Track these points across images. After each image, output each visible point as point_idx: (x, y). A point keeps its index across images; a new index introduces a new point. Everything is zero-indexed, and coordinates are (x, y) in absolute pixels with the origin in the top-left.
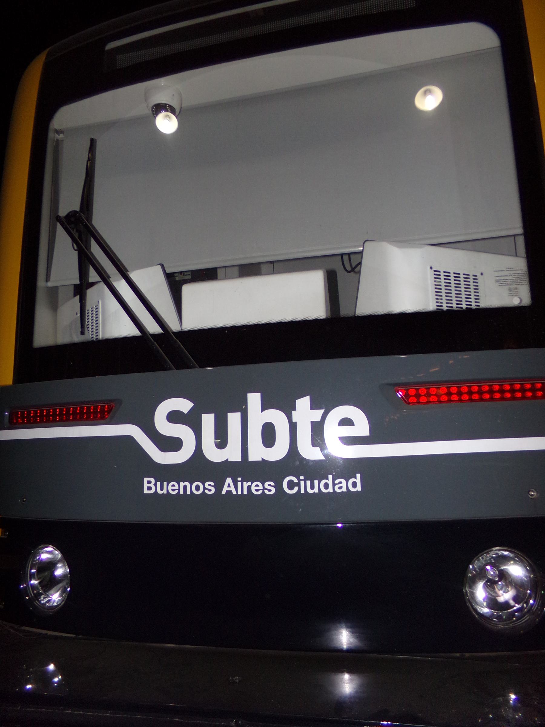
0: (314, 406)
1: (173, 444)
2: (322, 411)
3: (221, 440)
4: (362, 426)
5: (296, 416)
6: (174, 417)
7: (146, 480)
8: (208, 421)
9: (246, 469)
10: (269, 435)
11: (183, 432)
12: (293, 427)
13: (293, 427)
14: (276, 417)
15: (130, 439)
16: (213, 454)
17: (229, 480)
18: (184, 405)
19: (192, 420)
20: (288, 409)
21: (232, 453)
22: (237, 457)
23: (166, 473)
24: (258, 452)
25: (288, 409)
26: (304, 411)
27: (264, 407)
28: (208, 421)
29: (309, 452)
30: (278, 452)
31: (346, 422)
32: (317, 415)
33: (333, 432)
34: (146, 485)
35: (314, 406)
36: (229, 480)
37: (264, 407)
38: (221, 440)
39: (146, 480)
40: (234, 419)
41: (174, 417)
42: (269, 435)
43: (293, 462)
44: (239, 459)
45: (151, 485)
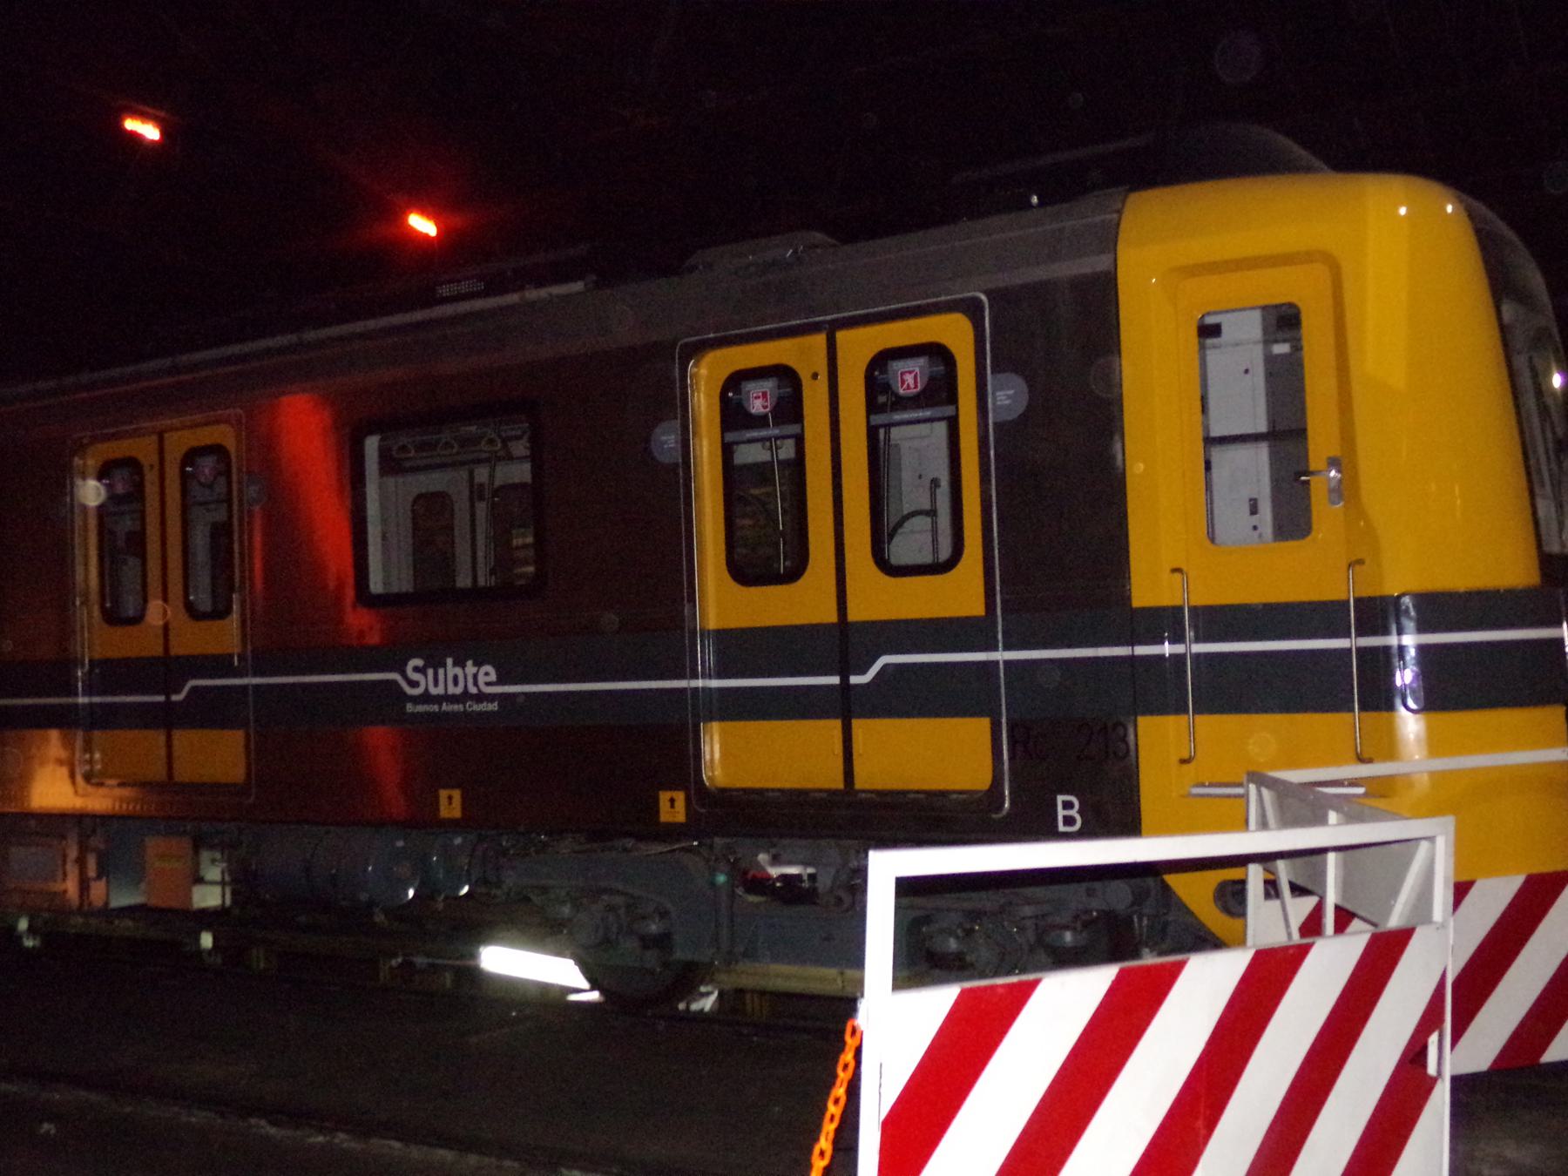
1: (414, 684)
3: (436, 683)
4: (493, 677)
6: (416, 669)
8: (430, 672)
9: (448, 698)
14: (458, 671)
15: (395, 682)
16: (433, 691)
18: (418, 662)
21: (440, 690)
24: (452, 690)
26: (470, 668)
28: (430, 672)
29: (473, 690)
30: (459, 690)
31: (487, 674)
33: (482, 679)
38: (436, 683)
40: (441, 671)
41: (416, 669)
42: (456, 682)
43: (466, 695)
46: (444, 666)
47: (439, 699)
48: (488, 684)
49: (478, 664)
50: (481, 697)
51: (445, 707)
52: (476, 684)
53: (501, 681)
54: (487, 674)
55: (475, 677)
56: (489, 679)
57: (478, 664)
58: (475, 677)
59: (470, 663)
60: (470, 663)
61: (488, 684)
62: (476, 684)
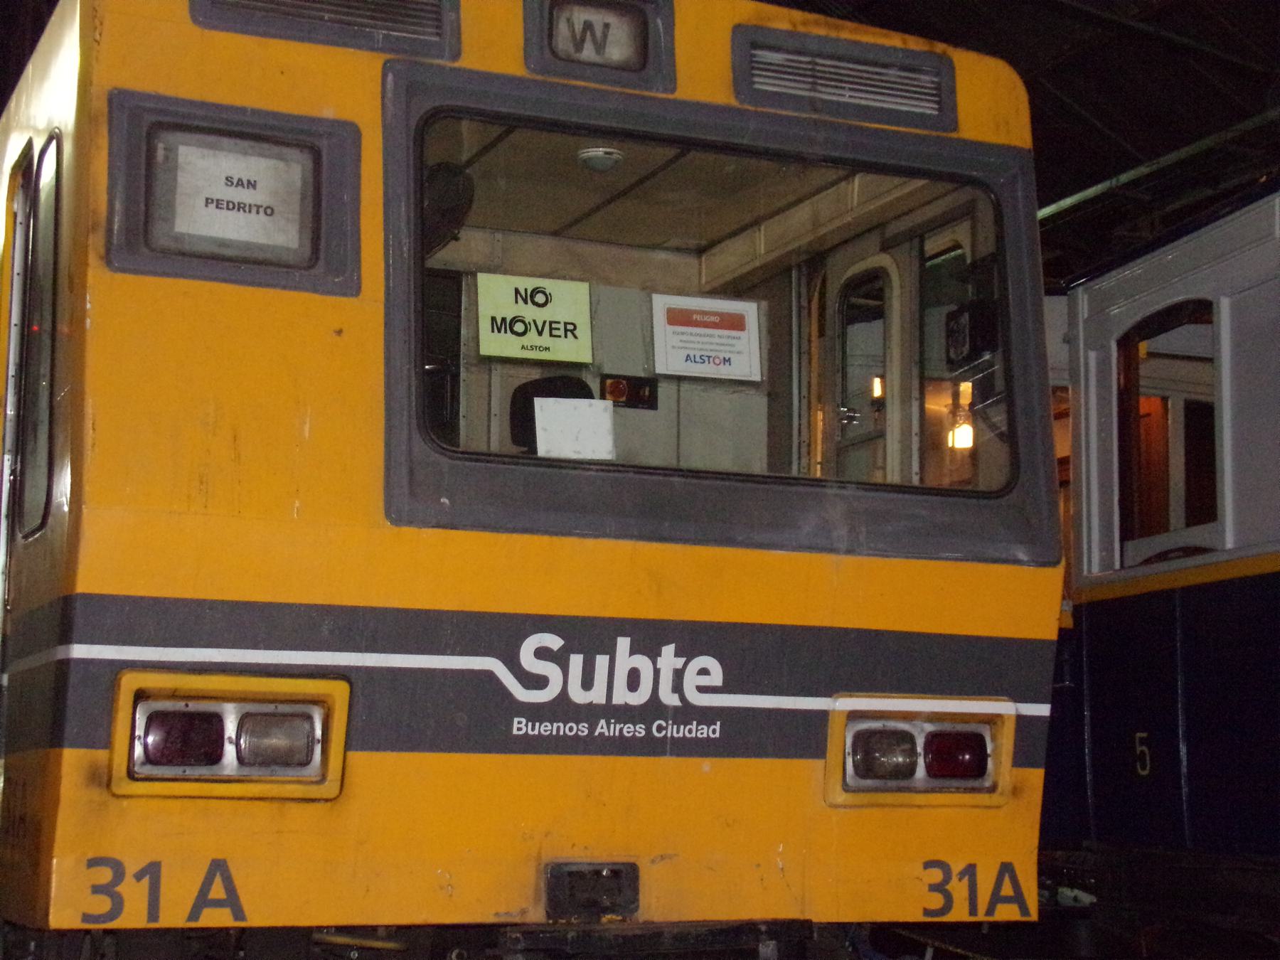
0: (677, 655)
1: (539, 682)
2: (684, 660)
3: (587, 684)
4: (716, 678)
5: (661, 662)
6: (542, 653)
7: (516, 720)
8: (576, 661)
10: (633, 680)
11: (549, 669)
12: (657, 672)
13: (657, 672)
14: (642, 663)
15: (489, 676)
16: (578, 695)
17: (603, 722)
19: (559, 657)
20: (654, 655)
21: (597, 695)
22: (601, 700)
23: (535, 712)
24: (621, 696)
25: (654, 655)
26: (669, 658)
27: (632, 653)
28: (576, 661)
29: (669, 698)
30: (640, 697)
31: (704, 672)
32: (680, 662)
33: (691, 680)
34: (515, 726)
35: (677, 655)
36: (603, 722)
37: (632, 653)
38: (587, 684)
39: (516, 720)
40: (602, 661)
41: (542, 653)
42: (633, 680)
43: (654, 708)
44: (603, 701)
45: (522, 726)
46: (611, 652)
47: (590, 713)
48: (701, 689)
49: (689, 652)
50: (686, 713)
51: (602, 728)
52: (678, 687)
53: (725, 689)
54: (704, 672)
55: (679, 675)
56: (704, 681)
57: (689, 652)
58: (679, 675)
59: (668, 650)
60: (668, 650)
61: (702, 689)
62: (678, 687)
